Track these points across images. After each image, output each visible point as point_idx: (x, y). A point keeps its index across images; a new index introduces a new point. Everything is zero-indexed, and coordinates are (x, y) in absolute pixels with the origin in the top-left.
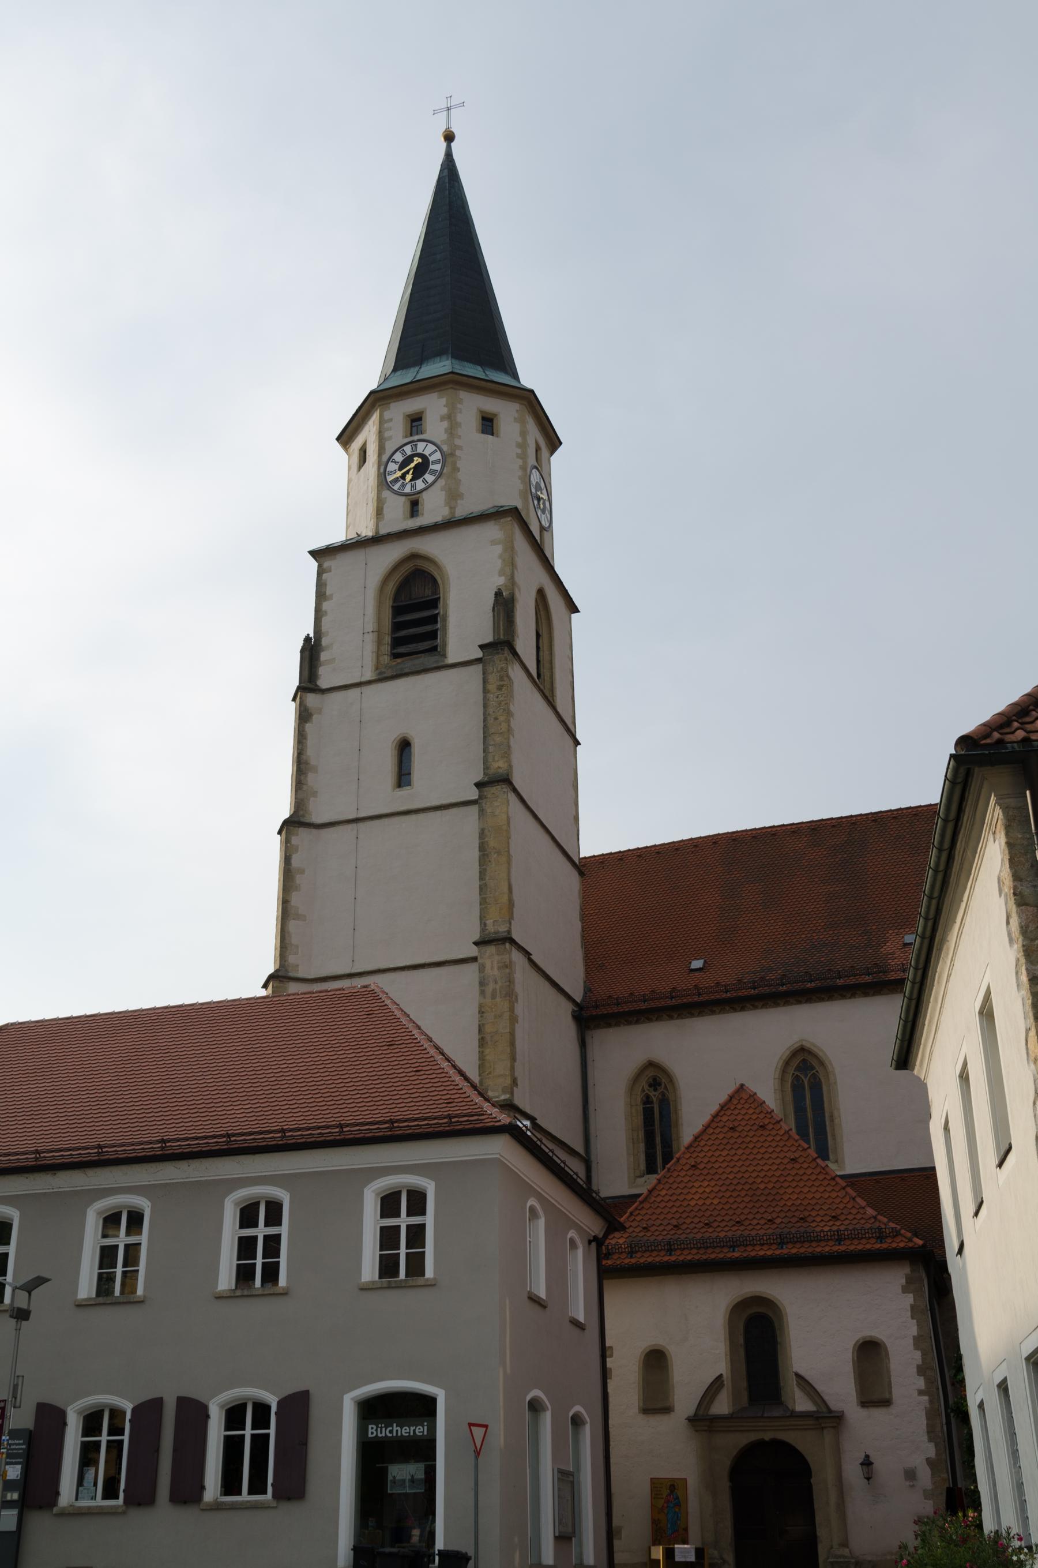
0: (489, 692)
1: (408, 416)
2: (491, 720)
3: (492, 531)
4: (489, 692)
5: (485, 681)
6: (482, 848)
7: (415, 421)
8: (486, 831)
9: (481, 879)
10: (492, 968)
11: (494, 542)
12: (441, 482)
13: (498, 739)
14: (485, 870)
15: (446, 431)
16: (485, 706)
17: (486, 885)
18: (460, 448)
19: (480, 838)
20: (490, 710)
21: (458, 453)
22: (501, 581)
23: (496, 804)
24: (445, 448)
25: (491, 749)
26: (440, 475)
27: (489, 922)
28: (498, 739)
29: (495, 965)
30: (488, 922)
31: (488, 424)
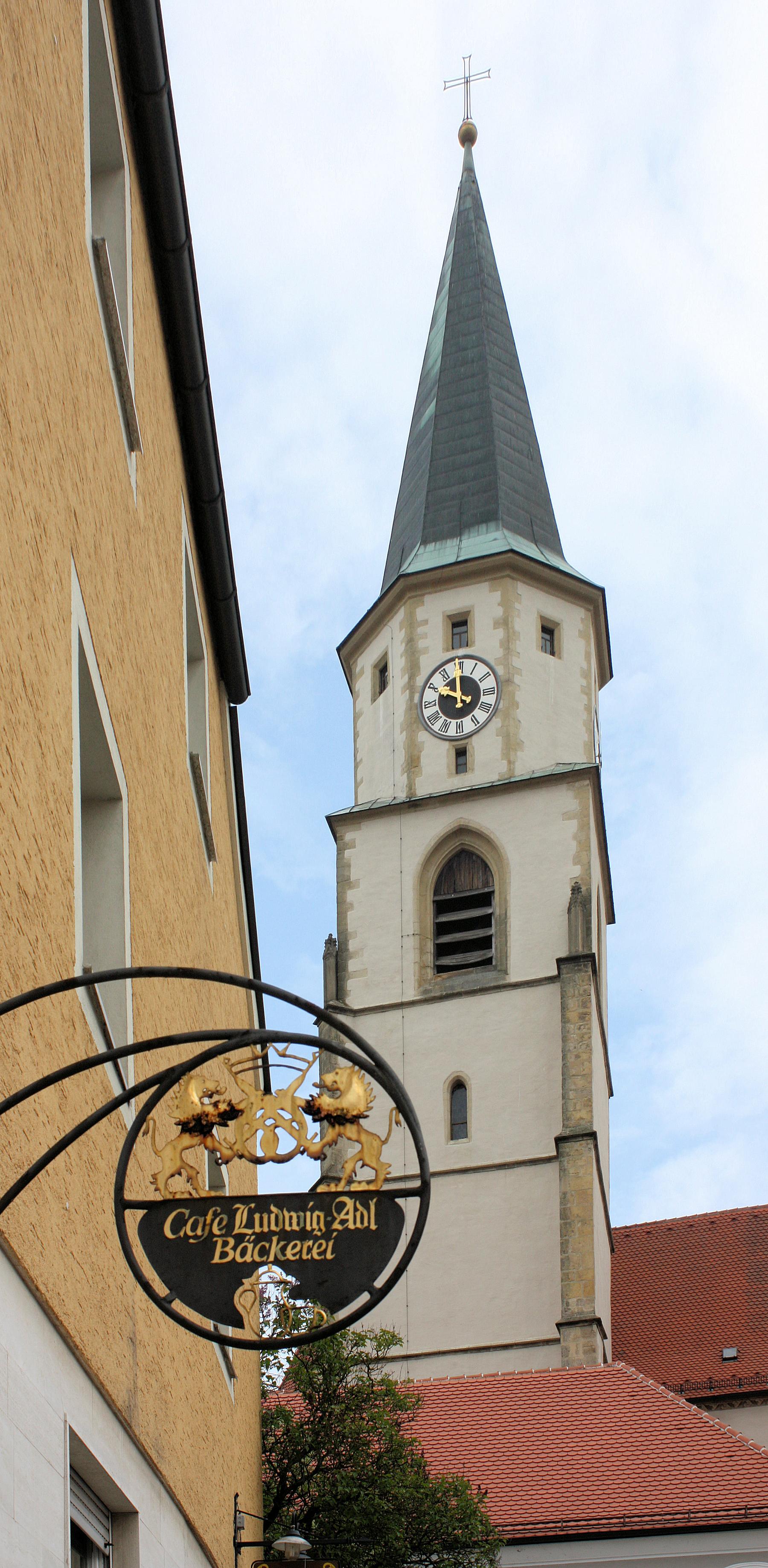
0: (569, 1021)
1: (449, 617)
2: (571, 1058)
3: (567, 799)
4: (569, 1021)
5: (564, 1008)
6: (564, 1215)
7: (459, 624)
8: (568, 1195)
9: (563, 1251)
10: (577, 1352)
11: (567, 816)
12: (497, 722)
13: (580, 1082)
14: (567, 1241)
15: (502, 644)
16: (564, 1039)
17: (568, 1258)
18: (519, 671)
19: (561, 1203)
20: (571, 1046)
21: (517, 679)
22: (576, 871)
23: (580, 1163)
24: (500, 670)
25: (571, 1095)
26: (494, 712)
27: (572, 1301)
28: (580, 1082)
29: (581, 1351)
30: (570, 1301)
31: (549, 631)
